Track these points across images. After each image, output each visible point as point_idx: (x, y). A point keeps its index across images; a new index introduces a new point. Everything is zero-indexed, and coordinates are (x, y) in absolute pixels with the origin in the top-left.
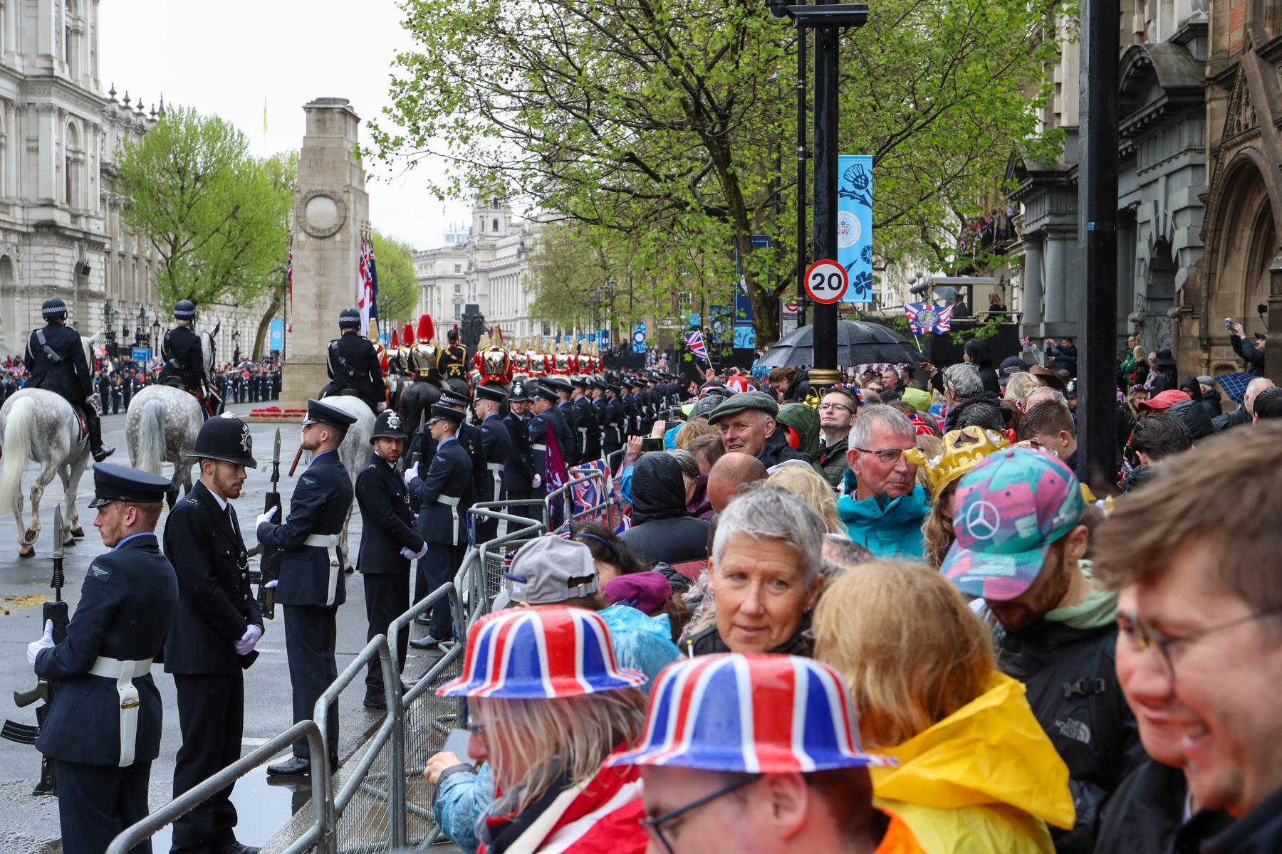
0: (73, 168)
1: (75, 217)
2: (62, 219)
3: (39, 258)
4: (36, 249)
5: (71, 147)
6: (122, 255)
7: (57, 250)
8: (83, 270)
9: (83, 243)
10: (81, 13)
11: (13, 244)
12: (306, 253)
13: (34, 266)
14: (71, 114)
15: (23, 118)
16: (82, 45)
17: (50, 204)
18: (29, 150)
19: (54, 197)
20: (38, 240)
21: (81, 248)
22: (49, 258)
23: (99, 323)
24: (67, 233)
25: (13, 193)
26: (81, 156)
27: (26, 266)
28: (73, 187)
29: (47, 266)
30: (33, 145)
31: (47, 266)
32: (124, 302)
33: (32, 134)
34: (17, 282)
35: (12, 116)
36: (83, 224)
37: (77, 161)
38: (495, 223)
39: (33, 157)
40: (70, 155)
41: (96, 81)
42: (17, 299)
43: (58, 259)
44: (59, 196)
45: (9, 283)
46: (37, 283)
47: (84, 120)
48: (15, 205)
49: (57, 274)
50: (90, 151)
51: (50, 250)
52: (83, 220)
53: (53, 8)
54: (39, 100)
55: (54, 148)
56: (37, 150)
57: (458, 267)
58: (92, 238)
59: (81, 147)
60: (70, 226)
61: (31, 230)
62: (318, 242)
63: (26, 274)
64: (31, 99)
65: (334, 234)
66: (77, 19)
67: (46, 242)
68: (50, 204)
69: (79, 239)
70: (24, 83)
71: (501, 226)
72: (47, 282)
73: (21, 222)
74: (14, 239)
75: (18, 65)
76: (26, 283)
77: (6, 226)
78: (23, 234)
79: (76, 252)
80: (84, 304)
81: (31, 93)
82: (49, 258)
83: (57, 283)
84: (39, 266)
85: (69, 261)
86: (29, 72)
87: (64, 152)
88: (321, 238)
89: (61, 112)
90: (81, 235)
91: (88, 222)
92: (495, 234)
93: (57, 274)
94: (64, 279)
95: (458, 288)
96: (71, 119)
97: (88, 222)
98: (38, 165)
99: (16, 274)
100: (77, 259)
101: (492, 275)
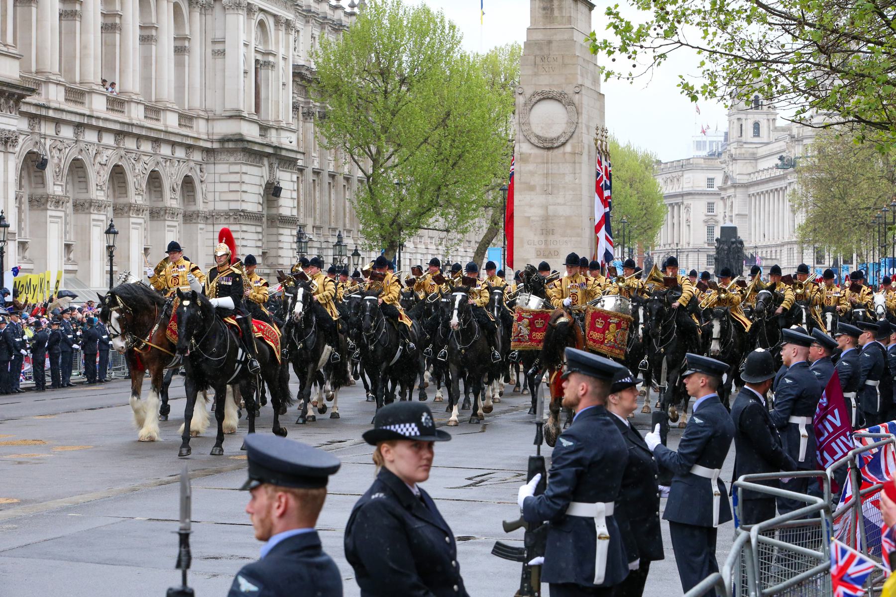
0: (262, 72)
1: (264, 129)
2: (251, 132)
3: (224, 178)
4: (221, 168)
5: (261, 48)
6: (317, 173)
7: (245, 168)
8: (273, 191)
9: (273, 160)
11: (197, 163)
12: (531, 167)
14: (261, 10)
15: (208, 17)
17: (237, 116)
18: (216, 53)
19: (242, 108)
20: (224, 157)
21: (271, 166)
22: (236, 178)
23: (290, 253)
24: (256, 148)
25: (196, 104)
26: (271, 59)
27: (211, 187)
28: (263, 95)
29: (234, 187)
30: (219, 47)
31: (234, 187)
32: (319, 228)
33: (219, 35)
34: (200, 206)
35: (197, 15)
36: (273, 137)
37: (267, 64)
38: (757, 126)
39: (219, 61)
40: (259, 57)
42: (200, 226)
43: (245, 178)
44: (247, 106)
45: (192, 208)
46: (223, 207)
47: (275, 16)
48: (198, 117)
49: (245, 197)
50: (282, 52)
51: (236, 168)
52: (273, 132)
55: (242, 49)
56: (223, 53)
57: (711, 181)
58: (284, 153)
59: (272, 48)
60: (259, 140)
61: (216, 146)
63: (210, 197)
65: (564, 144)
67: (232, 159)
68: (237, 116)
69: (268, 155)
71: (764, 130)
72: (234, 206)
73: (205, 137)
74: (197, 156)
76: (210, 207)
77: (190, 142)
79: (265, 171)
80: (274, 231)
82: (236, 178)
83: (244, 206)
84: (225, 187)
85: (257, 180)
87: (253, 53)
88: (549, 149)
90: (270, 151)
91: (279, 135)
92: (756, 140)
93: (245, 197)
94: (252, 203)
95: (711, 207)
96: (261, 16)
97: (279, 135)
98: (224, 70)
99: (199, 197)
100: (266, 179)
101: (752, 191)
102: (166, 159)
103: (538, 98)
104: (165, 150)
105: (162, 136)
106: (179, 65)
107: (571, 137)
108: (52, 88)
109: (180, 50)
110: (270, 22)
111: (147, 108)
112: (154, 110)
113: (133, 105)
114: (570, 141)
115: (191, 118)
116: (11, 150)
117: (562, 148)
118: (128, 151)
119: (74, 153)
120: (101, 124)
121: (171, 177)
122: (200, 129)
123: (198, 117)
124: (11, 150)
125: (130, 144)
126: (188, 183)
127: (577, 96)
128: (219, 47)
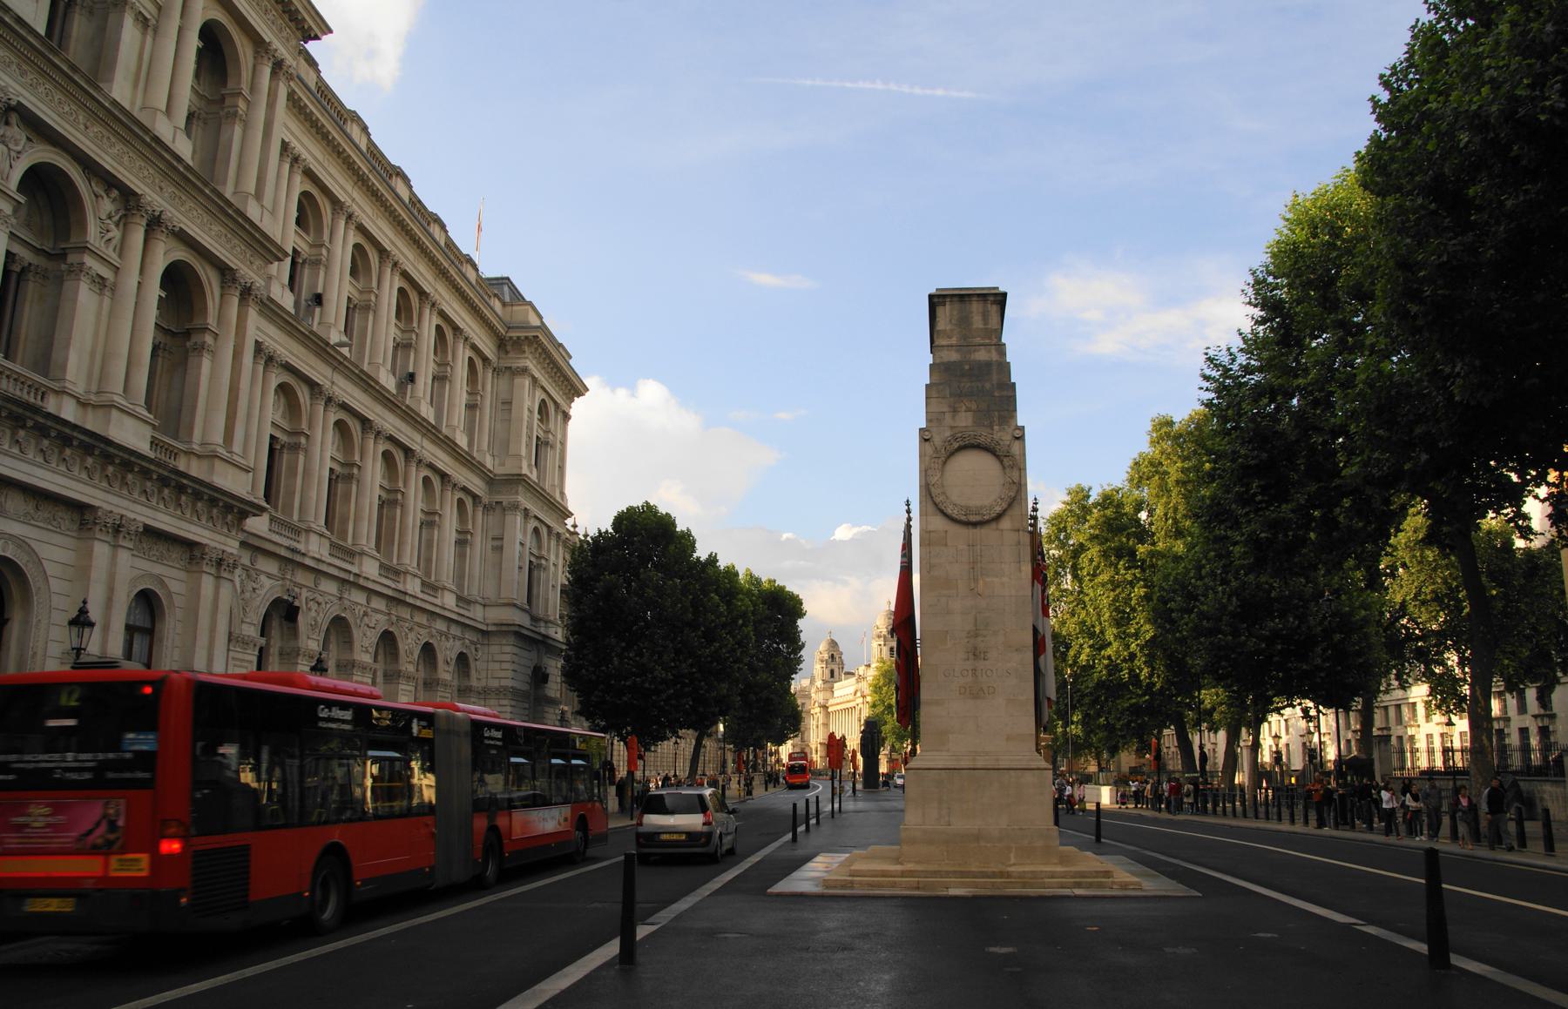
0: (535, 573)
1: (535, 619)
3: (497, 658)
4: (494, 649)
5: (535, 551)
10: (552, 426)
11: (472, 642)
13: (492, 666)
16: (550, 457)
18: (494, 548)
28: (535, 591)
30: (496, 543)
34: (474, 683)
37: (539, 566)
41: (562, 494)
44: (522, 599)
46: (494, 684)
47: (548, 527)
50: (552, 558)
51: (508, 649)
53: (526, 413)
54: (505, 499)
55: (518, 547)
56: (501, 548)
59: (544, 553)
62: (972, 532)
64: (499, 498)
65: (999, 517)
66: (547, 432)
70: (492, 481)
72: (504, 683)
75: (489, 462)
76: (483, 683)
78: (484, 633)
81: (499, 493)
84: (497, 666)
86: (499, 470)
88: (975, 524)
89: (526, 512)
99: (473, 673)
102: (441, 633)
103: (956, 445)
104: (440, 625)
105: (437, 610)
106: (461, 556)
107: (1010, 505)
108: (314, 538)
109: (462, 543)
110: (544, 531)
111: (423, 584)
112: (431, 587)
113: (409, 578)
114: (1009, 513)
115: (469, 602)
116: (225, 575)
117: (993, 525)
118: (399, 619)
119: (335, 611)
120: (371, 585)
121: (447, 650)
122: (477, 613)
123: (476, 602)
124: (225, 575)
125: (405, 613)
126: (462, 659)
127: (1017, 443)
128: (496, 543)
